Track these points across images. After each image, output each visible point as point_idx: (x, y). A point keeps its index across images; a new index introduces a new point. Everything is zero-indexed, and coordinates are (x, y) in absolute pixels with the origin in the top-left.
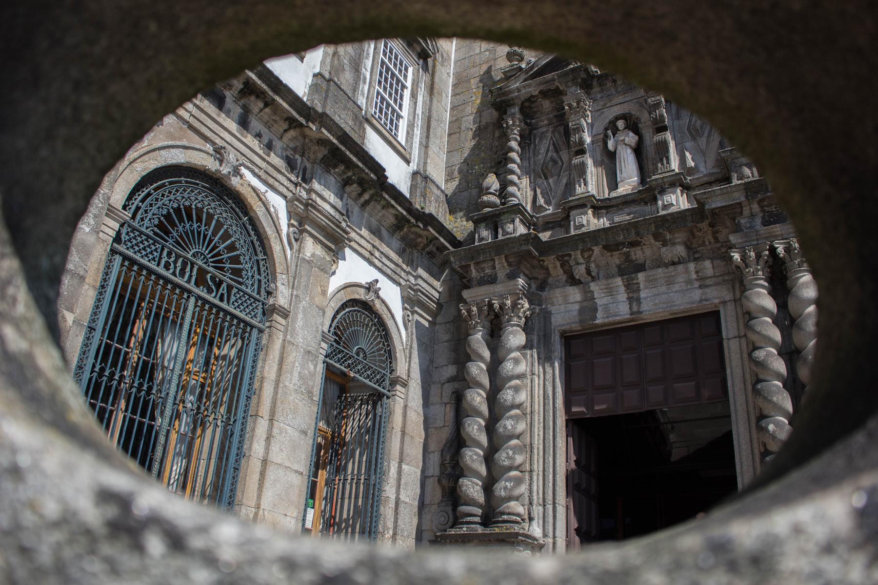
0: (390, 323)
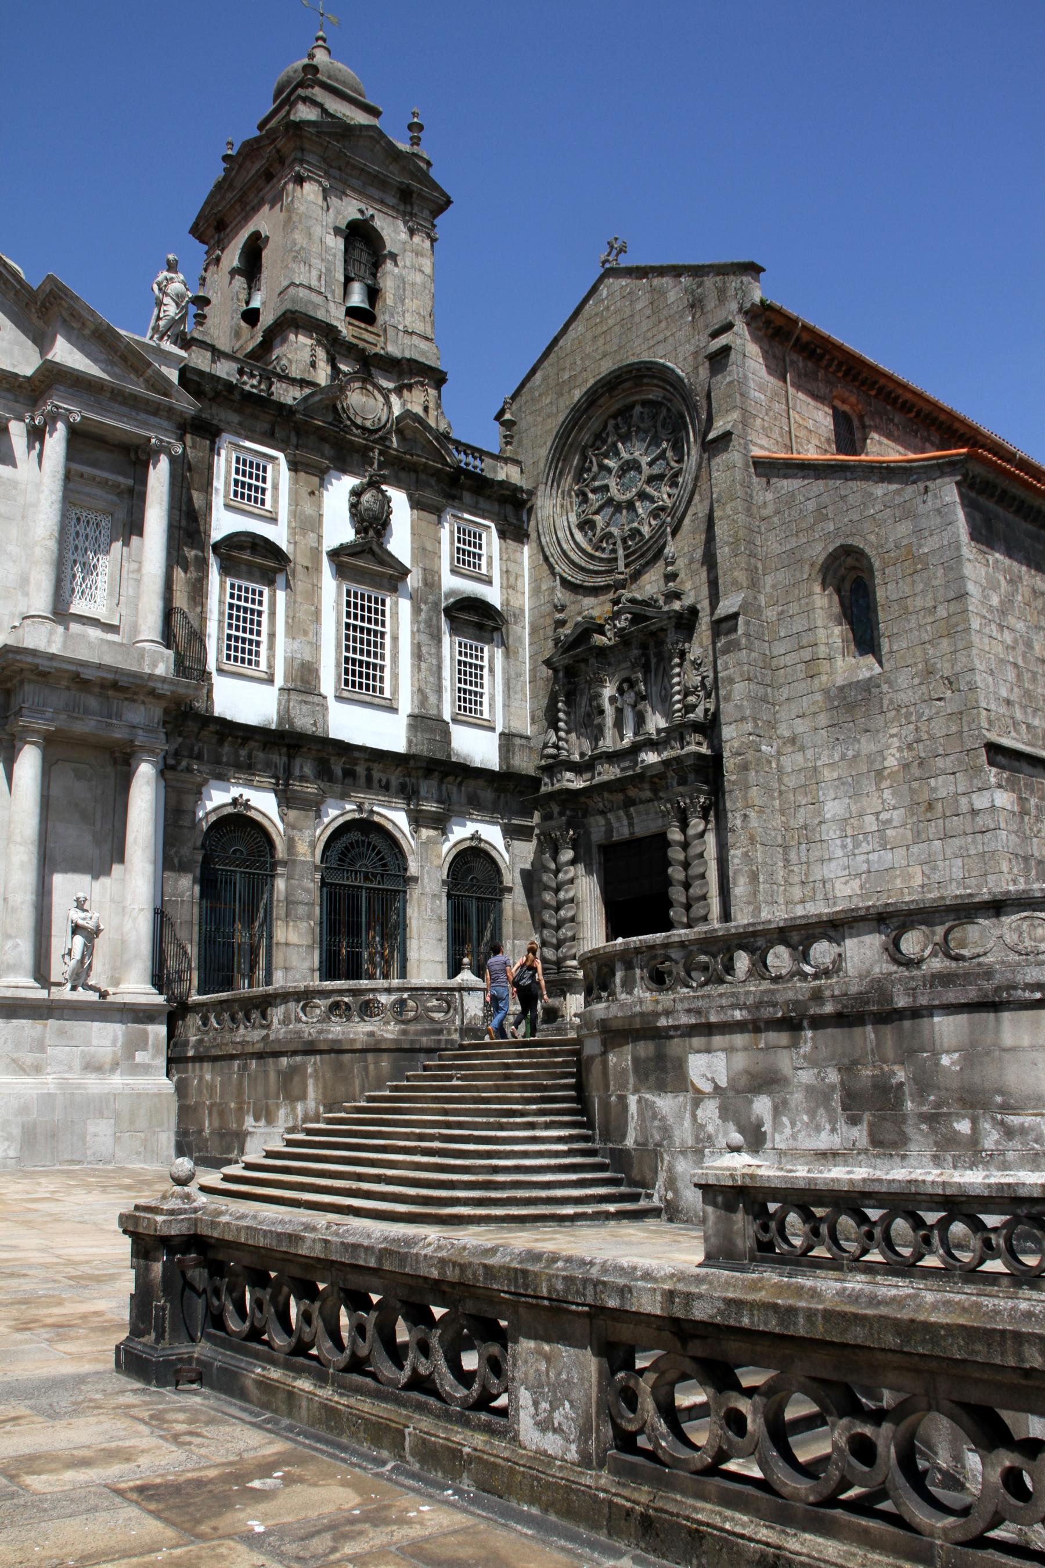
0: (494, 853)
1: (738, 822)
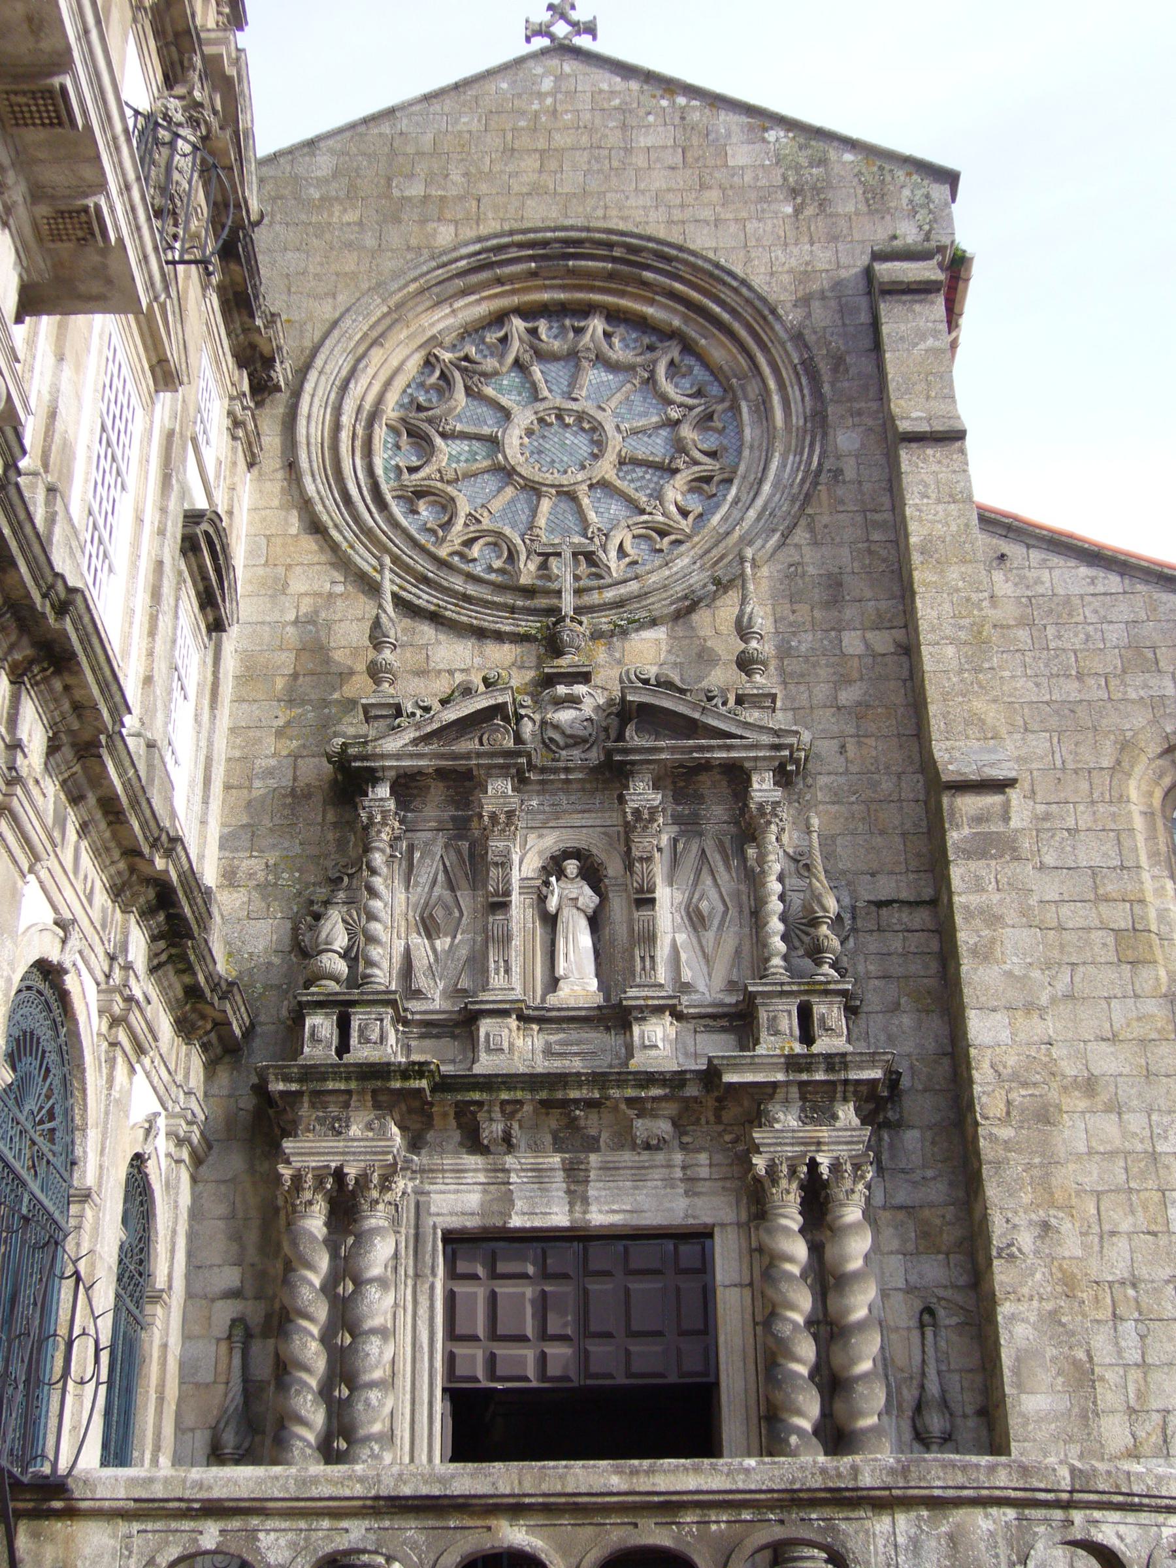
1: (1026, 1240)
